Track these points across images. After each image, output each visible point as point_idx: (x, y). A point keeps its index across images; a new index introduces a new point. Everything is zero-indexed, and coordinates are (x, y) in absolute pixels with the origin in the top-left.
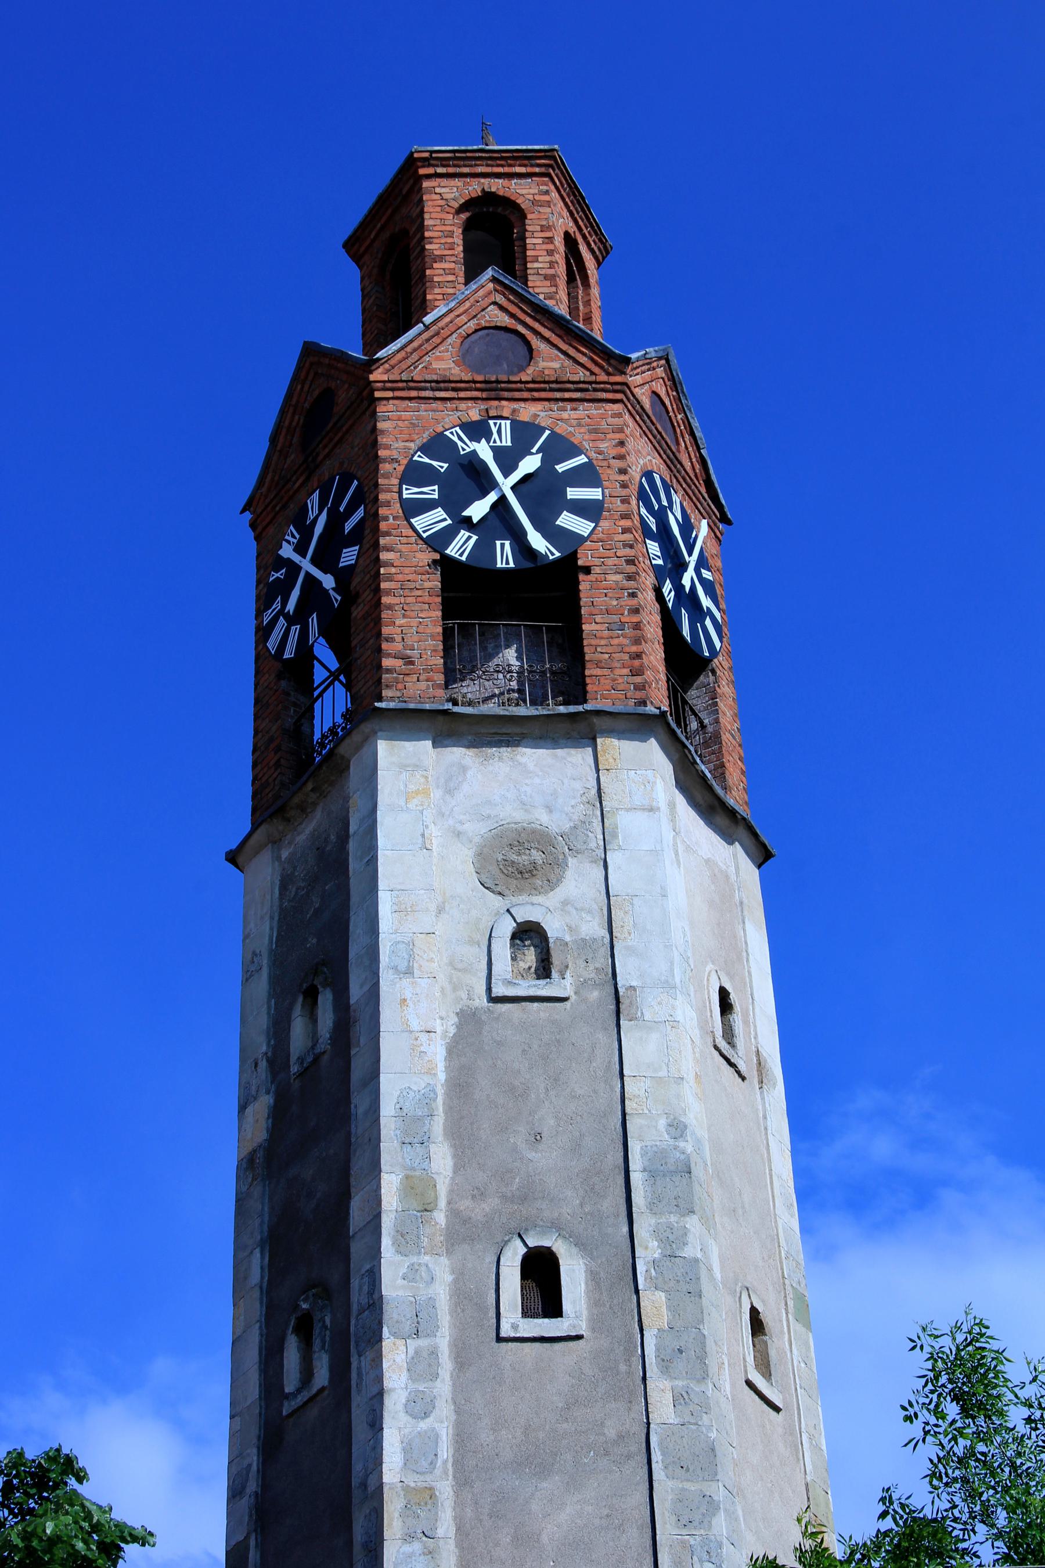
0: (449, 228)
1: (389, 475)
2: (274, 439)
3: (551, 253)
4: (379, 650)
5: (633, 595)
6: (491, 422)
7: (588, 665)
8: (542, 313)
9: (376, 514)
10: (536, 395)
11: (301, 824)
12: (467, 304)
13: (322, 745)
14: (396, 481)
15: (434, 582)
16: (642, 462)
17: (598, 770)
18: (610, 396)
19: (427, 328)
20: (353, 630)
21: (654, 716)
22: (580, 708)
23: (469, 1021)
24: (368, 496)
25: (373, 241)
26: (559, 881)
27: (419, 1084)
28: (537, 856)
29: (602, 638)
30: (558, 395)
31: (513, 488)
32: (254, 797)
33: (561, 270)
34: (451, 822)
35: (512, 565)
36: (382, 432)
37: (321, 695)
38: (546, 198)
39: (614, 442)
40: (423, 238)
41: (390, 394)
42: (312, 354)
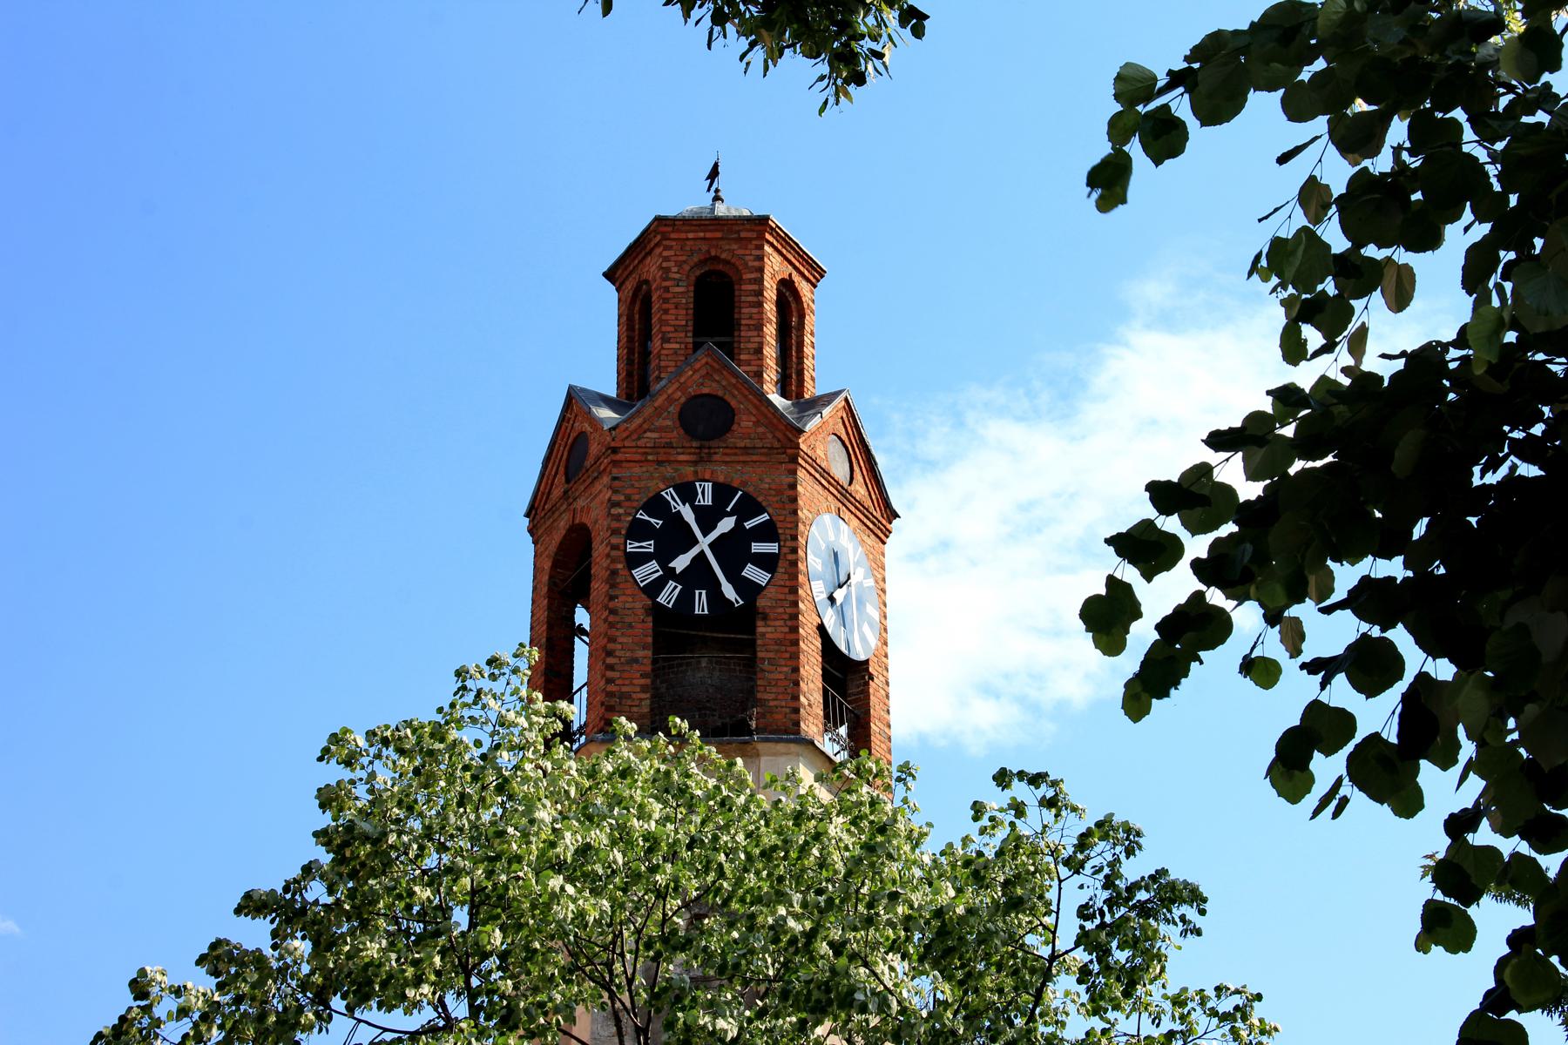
31: (711, 546)
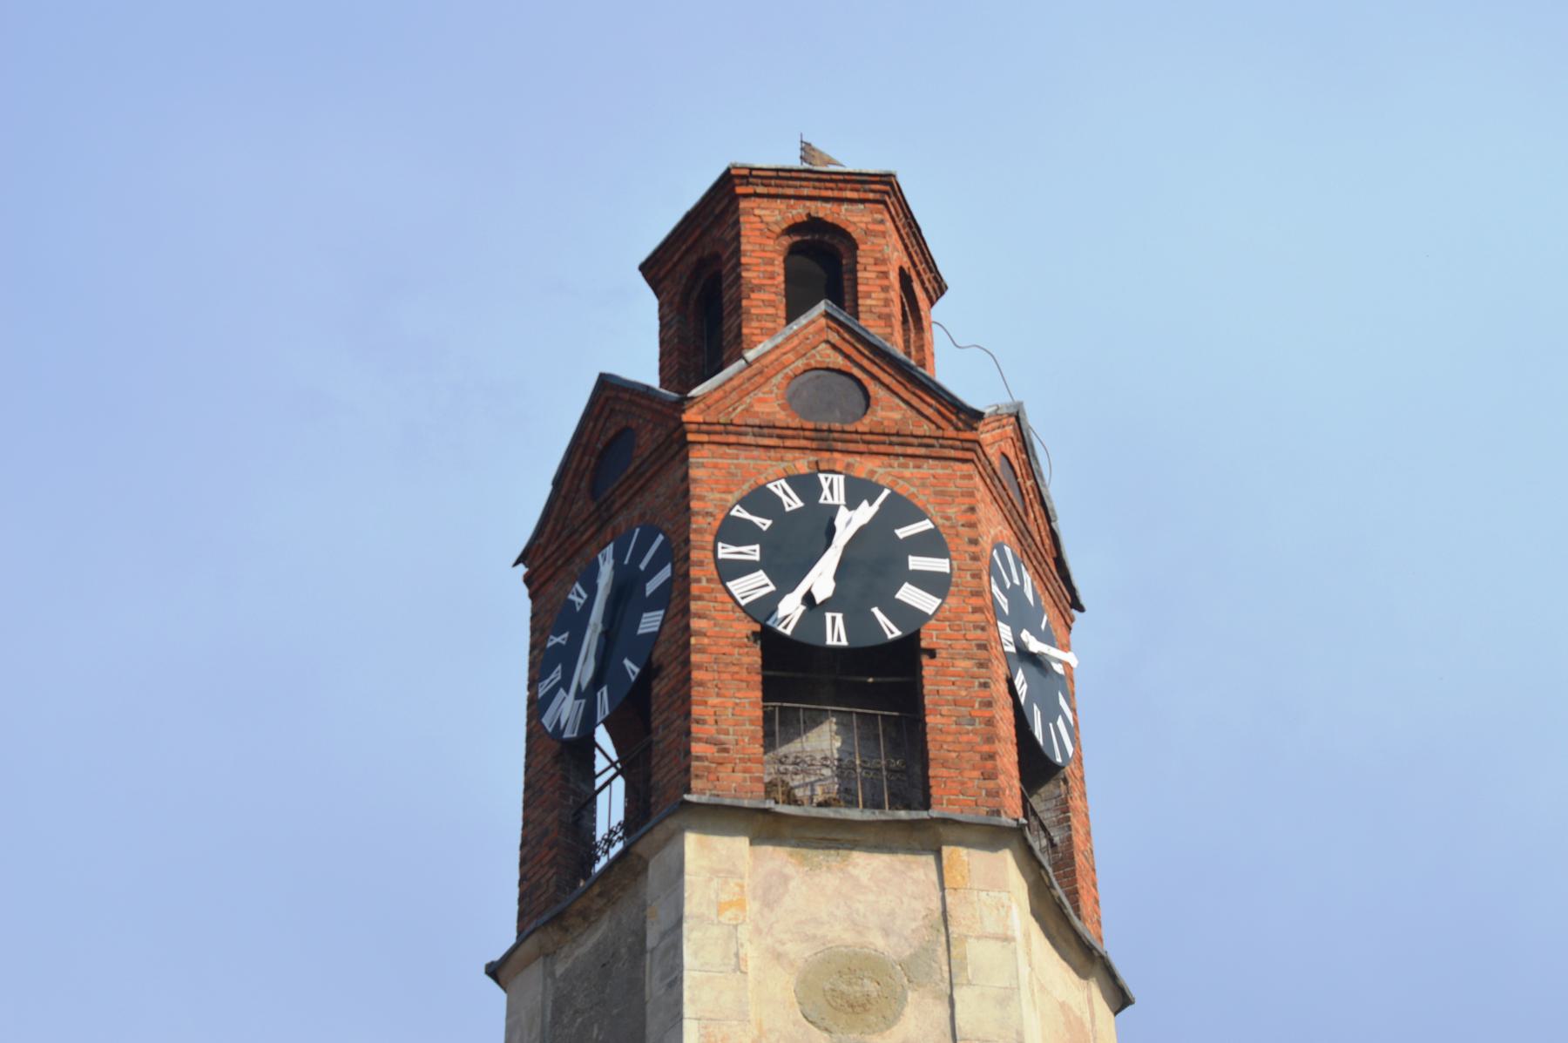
0: (769, 255)
1: (702, 527)
2: (558, 482)
3: (885, 289)
4: (688, 733)
5: (985, 685)
6: (822, 476)
7: (932, 764)
8: (881, 354)
9: (687, 574)
10: (874, 448)
11: (581, 934)
12: (796, 341)
13: (609, 842)
14: (710, 538)
15: (754, 656)
16: (992, 532)
17: (943, 889)
18: (960, 454)
19: (749, 364)
20: (654, 708)
21: (1010, 829)
22: (923, 815)
24: (677, 553)
25: (675, 265)
26: (897, 1016)
28: (871, 987)
29: (948, 733)
30: (898, 450)
32: (521, 900)
33: (896, 309)
34: (769, 940)
35: (844, 642)
36: (695, 481)
37: (608, 783)
38: (879, 227)
39: (964, 507)
40: (739, 264)
41: (705, 438)
42: (607, 386)
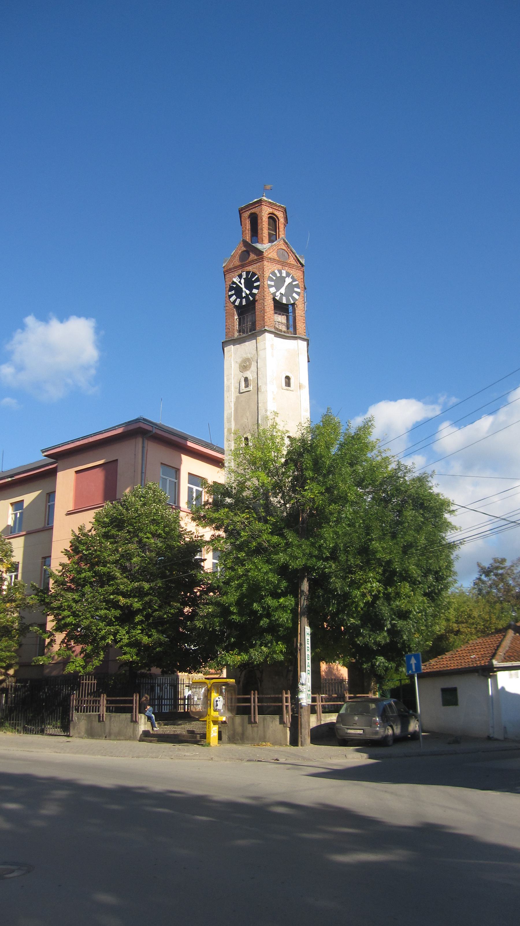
23: (237, 398)
27: (230, 412)
